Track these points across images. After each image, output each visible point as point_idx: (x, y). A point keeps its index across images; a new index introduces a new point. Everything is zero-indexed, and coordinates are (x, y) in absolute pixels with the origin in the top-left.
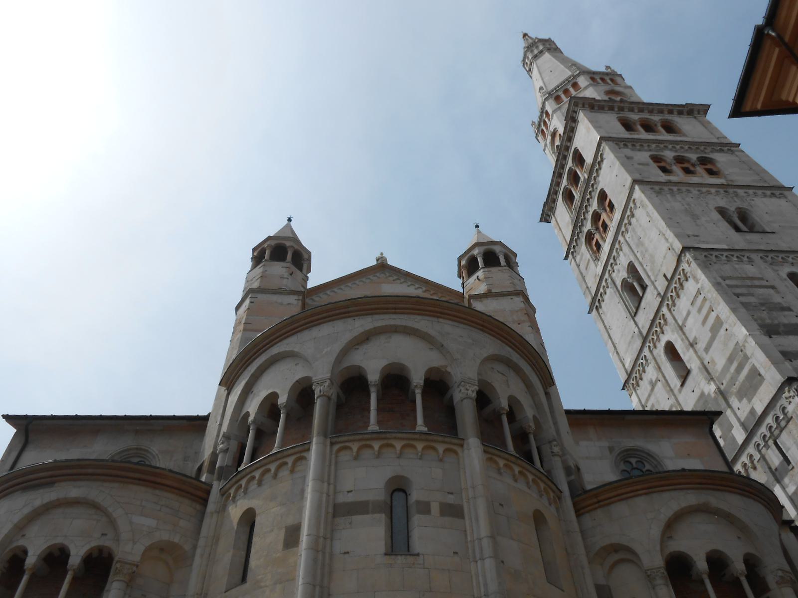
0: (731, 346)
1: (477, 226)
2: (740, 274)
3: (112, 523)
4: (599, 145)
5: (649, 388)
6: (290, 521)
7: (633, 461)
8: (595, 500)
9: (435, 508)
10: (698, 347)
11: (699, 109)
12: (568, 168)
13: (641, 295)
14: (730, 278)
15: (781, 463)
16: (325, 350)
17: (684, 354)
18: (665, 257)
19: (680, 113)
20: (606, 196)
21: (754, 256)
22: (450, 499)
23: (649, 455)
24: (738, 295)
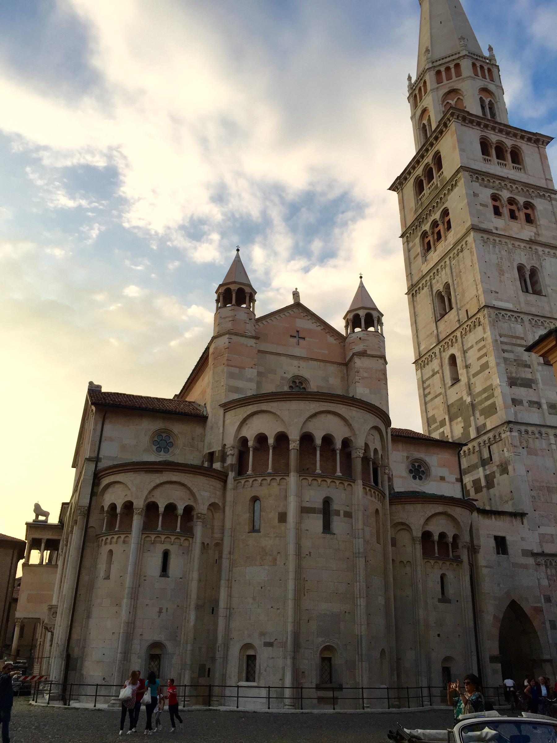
0: (488, 383)
1: (361, 277)
2: (512, 332)
3: (192, 494)
4: (458, 172)
5: (431, 373)
6: (280, 510)
7: (416, 464)
8: (399, 501)
9: (342, 513)
10: (470, 370)
11: (544, 140)
12: (426, 162)
13: (447, 312)
14: (505, 336)
15: (487, 458)
16: (295, 420)
17: (460, 369)
18: (471, 299)
19: (529, 140)
20: (448, 214)
21: (526, 318)
22: (348, 509)
23: (425, 463)
24: (504, 351)
